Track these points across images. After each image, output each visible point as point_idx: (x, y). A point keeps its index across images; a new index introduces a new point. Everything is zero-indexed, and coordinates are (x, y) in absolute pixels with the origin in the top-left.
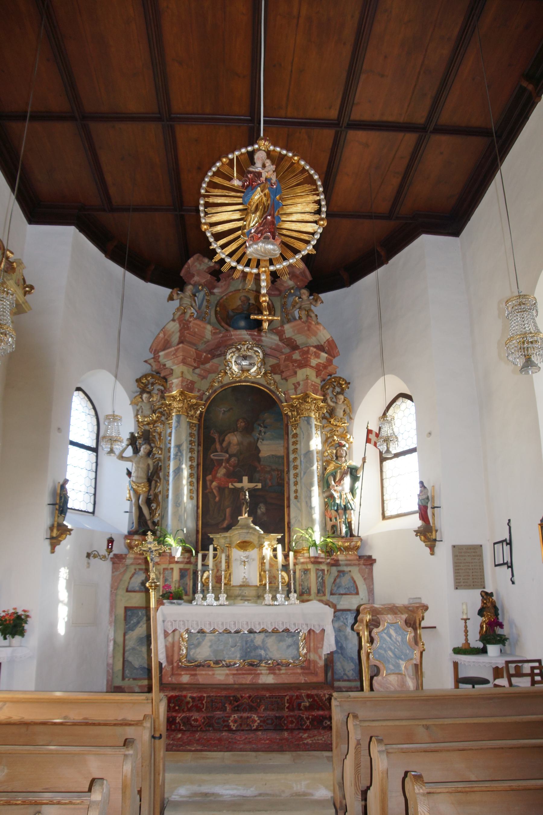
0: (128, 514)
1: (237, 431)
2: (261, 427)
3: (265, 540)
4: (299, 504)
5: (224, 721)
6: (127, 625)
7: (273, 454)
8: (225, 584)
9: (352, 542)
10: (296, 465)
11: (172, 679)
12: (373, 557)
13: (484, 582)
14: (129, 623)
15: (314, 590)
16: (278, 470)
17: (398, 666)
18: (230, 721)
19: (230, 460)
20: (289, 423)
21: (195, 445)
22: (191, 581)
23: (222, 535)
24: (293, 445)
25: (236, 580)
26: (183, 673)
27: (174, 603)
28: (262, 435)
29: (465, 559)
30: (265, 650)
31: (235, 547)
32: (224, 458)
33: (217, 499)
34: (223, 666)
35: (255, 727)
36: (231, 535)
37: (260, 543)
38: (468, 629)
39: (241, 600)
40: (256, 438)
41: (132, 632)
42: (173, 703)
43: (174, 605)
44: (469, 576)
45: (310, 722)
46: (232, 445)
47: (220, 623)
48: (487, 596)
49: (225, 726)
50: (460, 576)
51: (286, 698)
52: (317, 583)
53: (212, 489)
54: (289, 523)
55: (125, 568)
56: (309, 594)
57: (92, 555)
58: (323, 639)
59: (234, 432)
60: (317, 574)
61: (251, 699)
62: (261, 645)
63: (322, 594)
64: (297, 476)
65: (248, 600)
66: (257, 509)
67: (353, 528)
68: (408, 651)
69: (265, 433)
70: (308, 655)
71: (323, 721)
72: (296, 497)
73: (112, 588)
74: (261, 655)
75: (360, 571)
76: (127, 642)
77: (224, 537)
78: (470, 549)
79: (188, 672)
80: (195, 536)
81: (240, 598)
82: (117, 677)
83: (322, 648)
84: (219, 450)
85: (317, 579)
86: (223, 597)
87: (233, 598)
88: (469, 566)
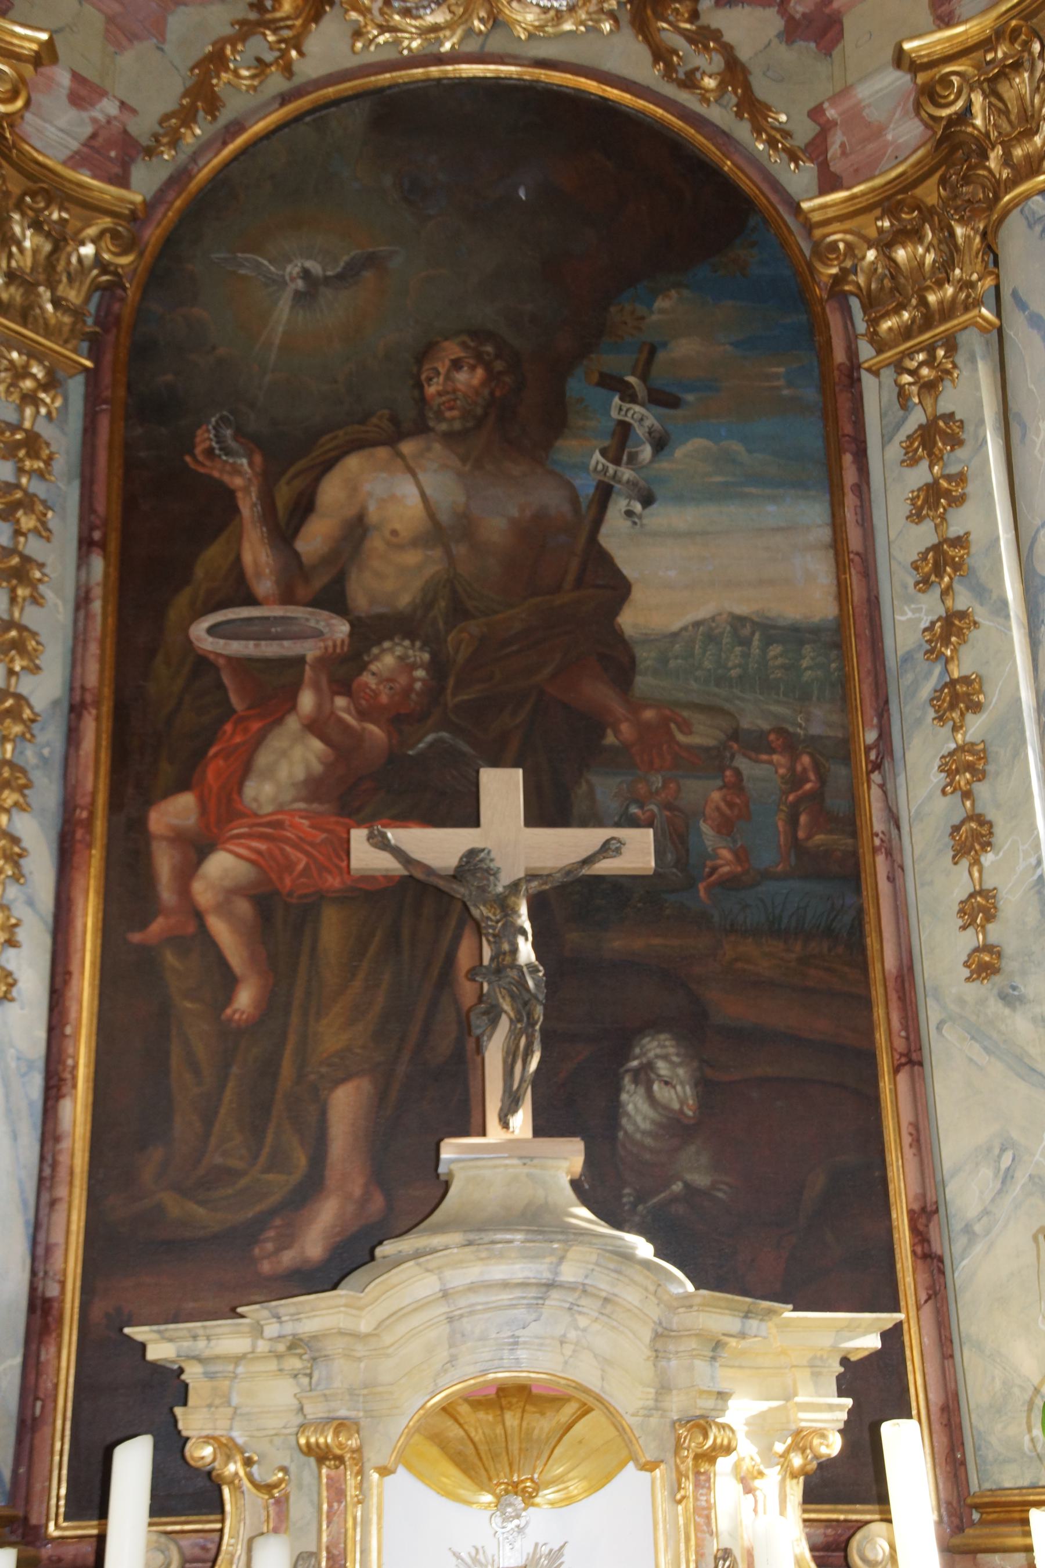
1: (421, 428)
2: (629, 395)
3: (724, 1377)
7: (742, 609)
10: (966, 680)
16: (791, 745)
19: (363, 667)
20: (866, 351)
21: (43, 531)
23: (272, 1329)
24: (916, 516)
28: (633, 458)
31: (405, 1458)
32: (310, 650)
33: (245, 999)
36: (364, 1326)
37: (677, 1405)
40: (586, 486)
46: (376, 543)
53: (198, 916)
59: (393, 438)
64: (980, 775)
66: (618, 1089)
69: (660, 444)
77: (295, 1344)
84: (264, 586)
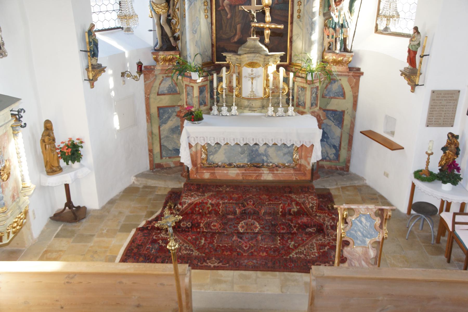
0: (152, 32)
4: (301, 23)
5: (234, 227)
6: (160, 120)
8: (236, 96)
9: (345, 57)
11: (197, 176)
12: (362, 70)
13: (453, 121)
14: (162, 118)
15: (308, 104)
17: (364, 242)
18: (239, 227)
22: (209, 94)
25: (246, 93)
26: (204, 171)
27: (195, 123)
29: (441, 103)
30: (266, 157)
33: (229, 16)
34: (235, 167)
35: (257, 231)
38: (430, 160)
39: (249, 110)
41: (165, 125)
42: (198, 208)
43: (195, 124)
44: (442, 116)
45: (297, 230)
47: (232, 139)
48: (453, 138)
49: (235, 230)
50: (433, 116)
51: (280, 206)
52: (311, 98)
53: (224, 7)
54: (291, 38)
55: (155, 77)
56: (304, 107)
57: (126, 75)
58: (312, 151)
60: (311, 92)
61: (254, 206)
62: (264, 153)
63: (315, 106)
65: (255, 111)
67: (347, 43)
68: (373, 233)
70: (300, 161)
71: (305, 229)
72: (299, 17)
73: (146, 94)
74: (263, 160)
75: (349, 81)
76: (161, 132)
78: (448, 94)
79: (208, 171)
80: (211, 50)
81: (248, 109)
82: (156, 157)
83: (311, 157)
85: (311, 95)
86: (234, 108)
87: (243, 108)
88: (443, 108)
